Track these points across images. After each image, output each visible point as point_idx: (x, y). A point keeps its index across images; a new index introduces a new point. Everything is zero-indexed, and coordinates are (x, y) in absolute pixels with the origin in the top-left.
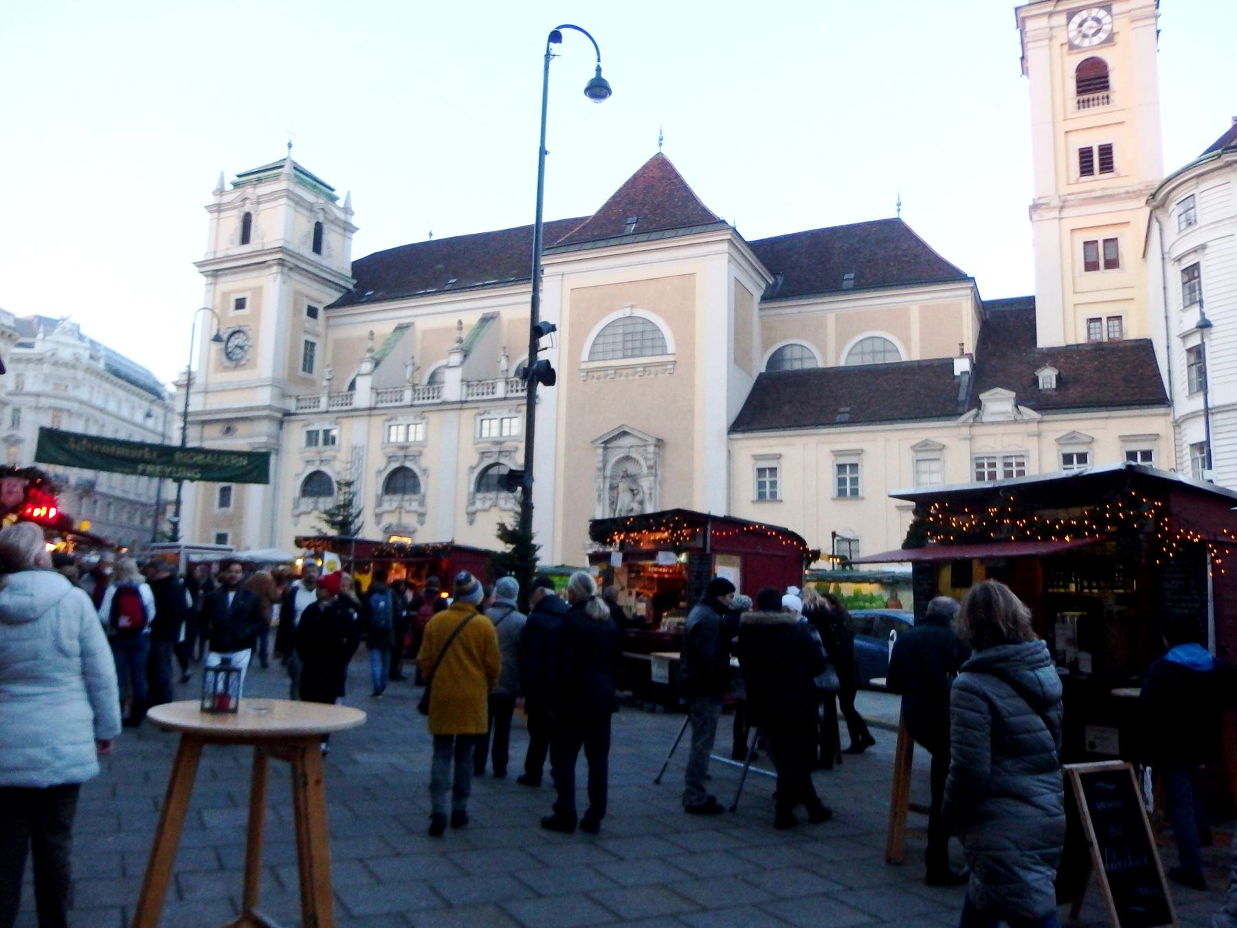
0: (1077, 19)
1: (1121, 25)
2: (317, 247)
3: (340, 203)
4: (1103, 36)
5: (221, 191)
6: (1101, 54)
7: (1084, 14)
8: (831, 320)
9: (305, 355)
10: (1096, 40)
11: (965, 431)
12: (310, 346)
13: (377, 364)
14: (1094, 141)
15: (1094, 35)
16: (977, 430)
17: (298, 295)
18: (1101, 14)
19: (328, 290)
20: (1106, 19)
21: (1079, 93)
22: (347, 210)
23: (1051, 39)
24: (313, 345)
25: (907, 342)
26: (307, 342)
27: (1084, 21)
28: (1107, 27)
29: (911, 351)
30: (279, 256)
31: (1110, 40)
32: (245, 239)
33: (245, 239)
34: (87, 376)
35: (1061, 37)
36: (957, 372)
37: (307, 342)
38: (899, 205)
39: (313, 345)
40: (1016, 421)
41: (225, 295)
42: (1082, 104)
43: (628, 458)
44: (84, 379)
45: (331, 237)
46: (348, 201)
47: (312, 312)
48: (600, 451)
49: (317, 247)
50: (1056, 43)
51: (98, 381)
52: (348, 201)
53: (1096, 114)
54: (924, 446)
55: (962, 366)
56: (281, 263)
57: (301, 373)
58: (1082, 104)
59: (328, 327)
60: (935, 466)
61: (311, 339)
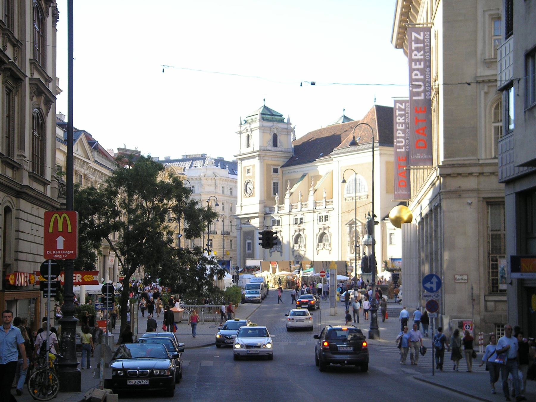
2: (275, 144)
3: (285, 121)
5: (241, 124)
9: (274, 188)
12: (276, 185)
17: (268, 166)
19: (282, 160)
22: (289, 123)
24: (277, 183)
26: (274, 183)
30: (258, 153)
32: (248, 147)
33: (248, 147)
34: (221, 182)
37: (274, 183)
41: (245, 167)
44: (220, 183)
45: (280, 138)
46: (289, 119)
47: (276, 171)
49: (275, 144)
51: (226, 183)
52: (289, 119)
56: (259, 156)
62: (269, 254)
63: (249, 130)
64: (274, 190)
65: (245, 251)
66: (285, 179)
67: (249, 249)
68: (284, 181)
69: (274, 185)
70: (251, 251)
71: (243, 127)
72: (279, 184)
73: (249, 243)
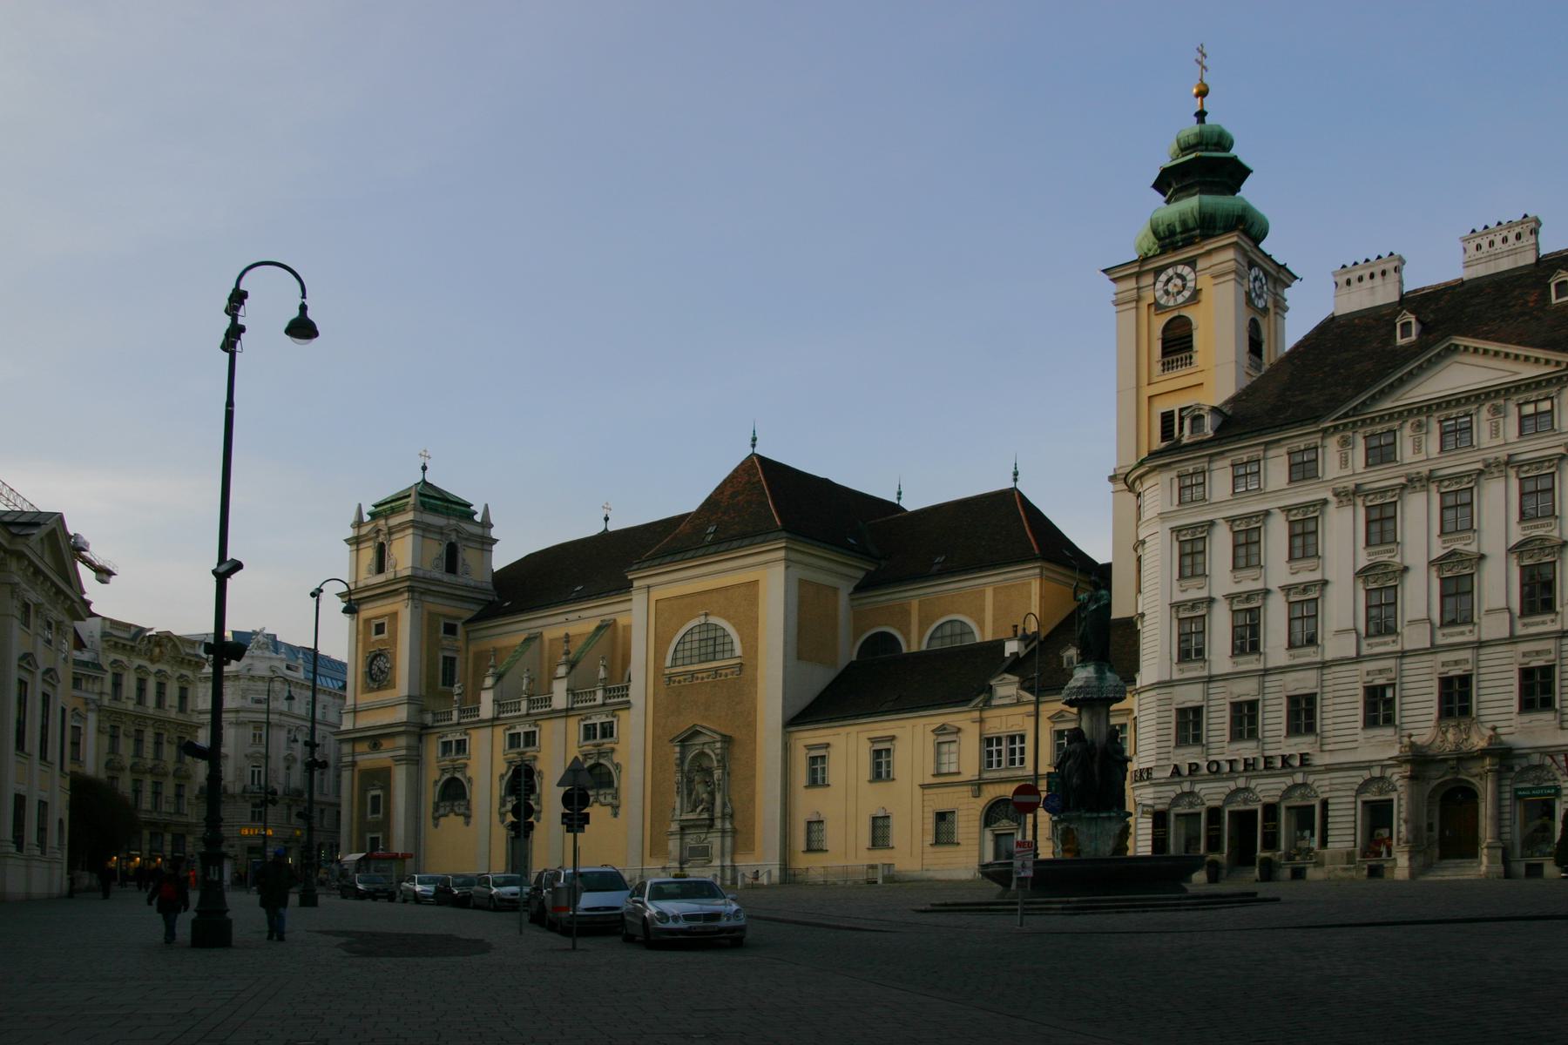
0: (1163, 277)
1: (1205, 282)
4: (1187, 294)
6: (1184, 312)
7: (1170, 272)
8: (915, 603)
10: (1180, 299)
11: (976, 714)
12: (450, 663)
13: (499, 677)
14: (1173, 404)
15: (1179, 293)
16: (986, 714)
18: (1185, 270)
20: (1192, 276)
21: (1164, 354)
23: (1138, 300)
24: (453, 659)
25: (982, 629)
26: (445, 658)
27: (1169, 281)
28: (1191, 284)
29: (984, 634)
31: (1195, 296)
35: (1148, 297)
36: (1007, 654)
37: (445, 658)
38: (1016, 474)
39: (453, 659)
40: (1019, 702)
42: (1167, 366)
43: (702, 754)
48: (677, 749)
50: (1143, 305)
53: (1179, 377)
54: (941, 730)
55: (1012, 647)
57: (440, 687)
58: (1167, 366)
59: (468, 640)
60: (953, 747)
61: (448, 654)
62: (430, 822)
63: (385, 530)
64: (444, 674)
65: (362, 815)
66: (472, 648)
67: (375, 810)
68: (471, 655)
69: (444, 664)
70: (381, 816)
71: (364, 530)
72: (458, 663)
73: (376, 798)
